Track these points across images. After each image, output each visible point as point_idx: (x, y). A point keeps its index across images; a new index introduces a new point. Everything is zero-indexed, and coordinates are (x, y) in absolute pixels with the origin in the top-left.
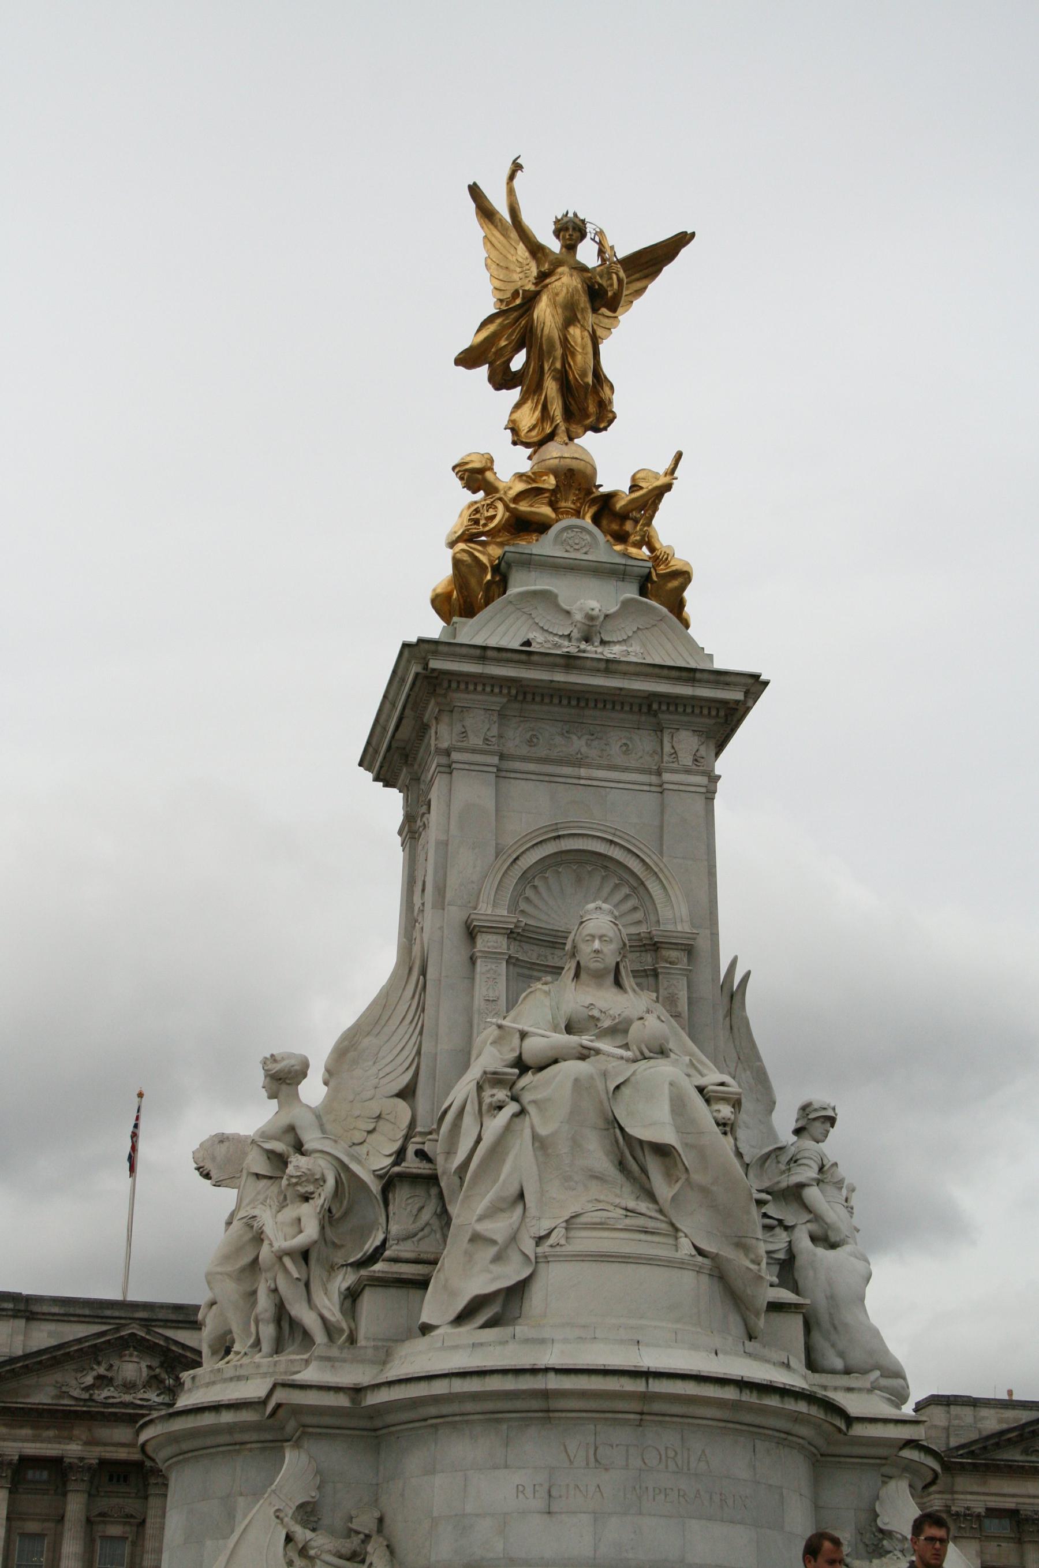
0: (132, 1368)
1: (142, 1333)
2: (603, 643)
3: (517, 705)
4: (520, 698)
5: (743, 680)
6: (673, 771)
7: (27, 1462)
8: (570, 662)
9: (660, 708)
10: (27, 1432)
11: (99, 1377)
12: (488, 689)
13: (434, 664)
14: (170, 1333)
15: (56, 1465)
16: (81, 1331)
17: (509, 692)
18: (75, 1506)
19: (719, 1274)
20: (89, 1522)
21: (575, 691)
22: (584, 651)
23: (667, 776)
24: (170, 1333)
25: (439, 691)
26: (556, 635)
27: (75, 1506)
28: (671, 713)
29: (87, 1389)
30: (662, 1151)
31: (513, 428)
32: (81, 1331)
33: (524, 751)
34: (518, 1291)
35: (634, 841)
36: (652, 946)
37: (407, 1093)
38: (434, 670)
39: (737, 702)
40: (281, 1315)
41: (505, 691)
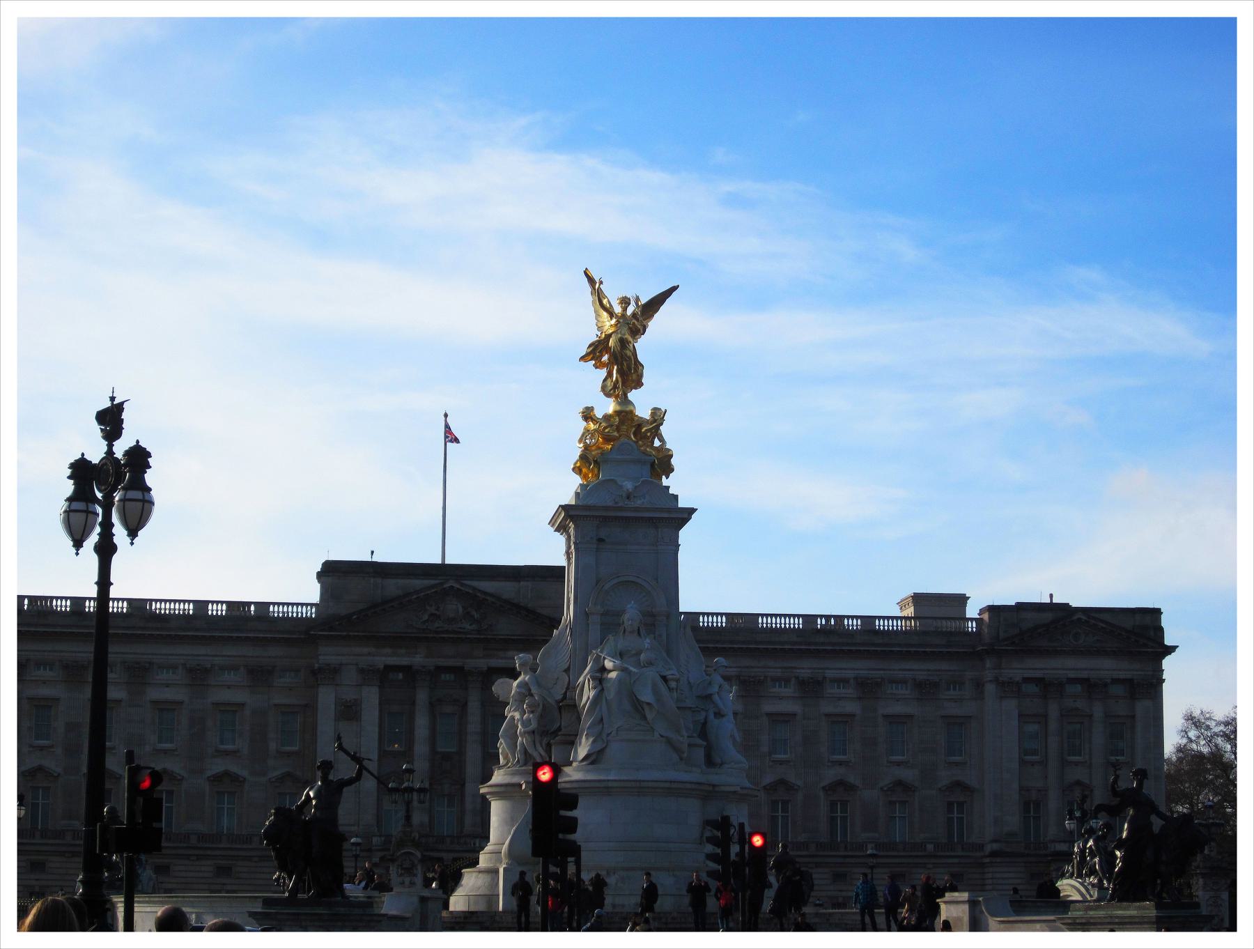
0: (453, 607)
1: (457, 586)
7: (389, 668)
8: (621, 509)
10: (388, 650)
11: (432, 615)
14: (475, 584)
15: (407, 669)
16: (418, 583)
18: (422, 696)
19: (669, 742)
20: (431, 703)
24: (475, 584)
27: (422, 696)
29: (425, 622)
30: (648, 704)
31: (603, 388)
32: (418, 583)
34: (601, 751)
36: (652, 615)
37: (567, 671)
40: (525, 752)
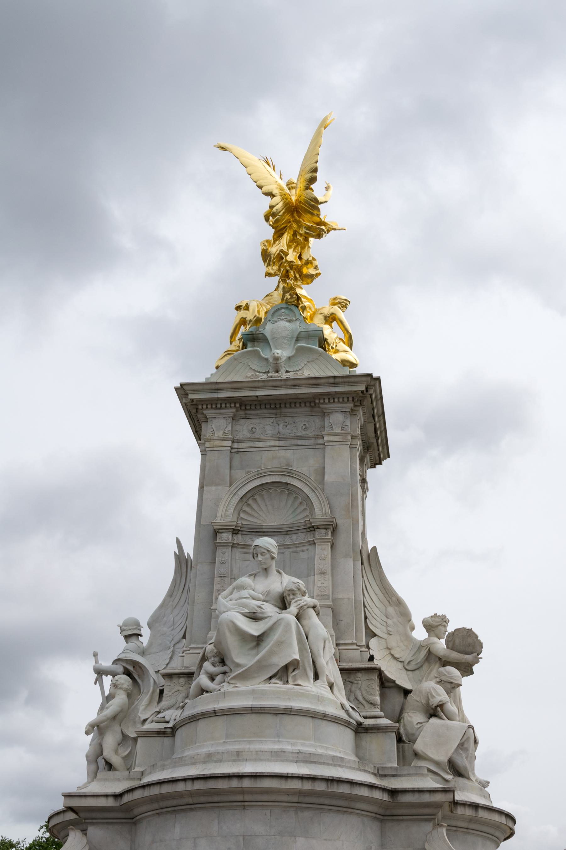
2: (287, 372)
3: (242, 413)
4: (243, 408)
5: (364, 379)
6: (329, 435)
8: (264, 384)
9: (319, 402)
12: (223, 405)
13: (191, 396)
17: (235, 406)
21: (269, 400)
22: (271, 377)
23: (326, 439)
25: (200, 411)
26: (257, 371)
28: (327, 403)
33: (248, 435)
35: (307, 478)
38: (192, 400)
39: (362, 392)
41: (233, 405)
